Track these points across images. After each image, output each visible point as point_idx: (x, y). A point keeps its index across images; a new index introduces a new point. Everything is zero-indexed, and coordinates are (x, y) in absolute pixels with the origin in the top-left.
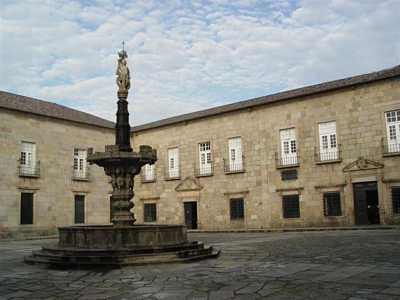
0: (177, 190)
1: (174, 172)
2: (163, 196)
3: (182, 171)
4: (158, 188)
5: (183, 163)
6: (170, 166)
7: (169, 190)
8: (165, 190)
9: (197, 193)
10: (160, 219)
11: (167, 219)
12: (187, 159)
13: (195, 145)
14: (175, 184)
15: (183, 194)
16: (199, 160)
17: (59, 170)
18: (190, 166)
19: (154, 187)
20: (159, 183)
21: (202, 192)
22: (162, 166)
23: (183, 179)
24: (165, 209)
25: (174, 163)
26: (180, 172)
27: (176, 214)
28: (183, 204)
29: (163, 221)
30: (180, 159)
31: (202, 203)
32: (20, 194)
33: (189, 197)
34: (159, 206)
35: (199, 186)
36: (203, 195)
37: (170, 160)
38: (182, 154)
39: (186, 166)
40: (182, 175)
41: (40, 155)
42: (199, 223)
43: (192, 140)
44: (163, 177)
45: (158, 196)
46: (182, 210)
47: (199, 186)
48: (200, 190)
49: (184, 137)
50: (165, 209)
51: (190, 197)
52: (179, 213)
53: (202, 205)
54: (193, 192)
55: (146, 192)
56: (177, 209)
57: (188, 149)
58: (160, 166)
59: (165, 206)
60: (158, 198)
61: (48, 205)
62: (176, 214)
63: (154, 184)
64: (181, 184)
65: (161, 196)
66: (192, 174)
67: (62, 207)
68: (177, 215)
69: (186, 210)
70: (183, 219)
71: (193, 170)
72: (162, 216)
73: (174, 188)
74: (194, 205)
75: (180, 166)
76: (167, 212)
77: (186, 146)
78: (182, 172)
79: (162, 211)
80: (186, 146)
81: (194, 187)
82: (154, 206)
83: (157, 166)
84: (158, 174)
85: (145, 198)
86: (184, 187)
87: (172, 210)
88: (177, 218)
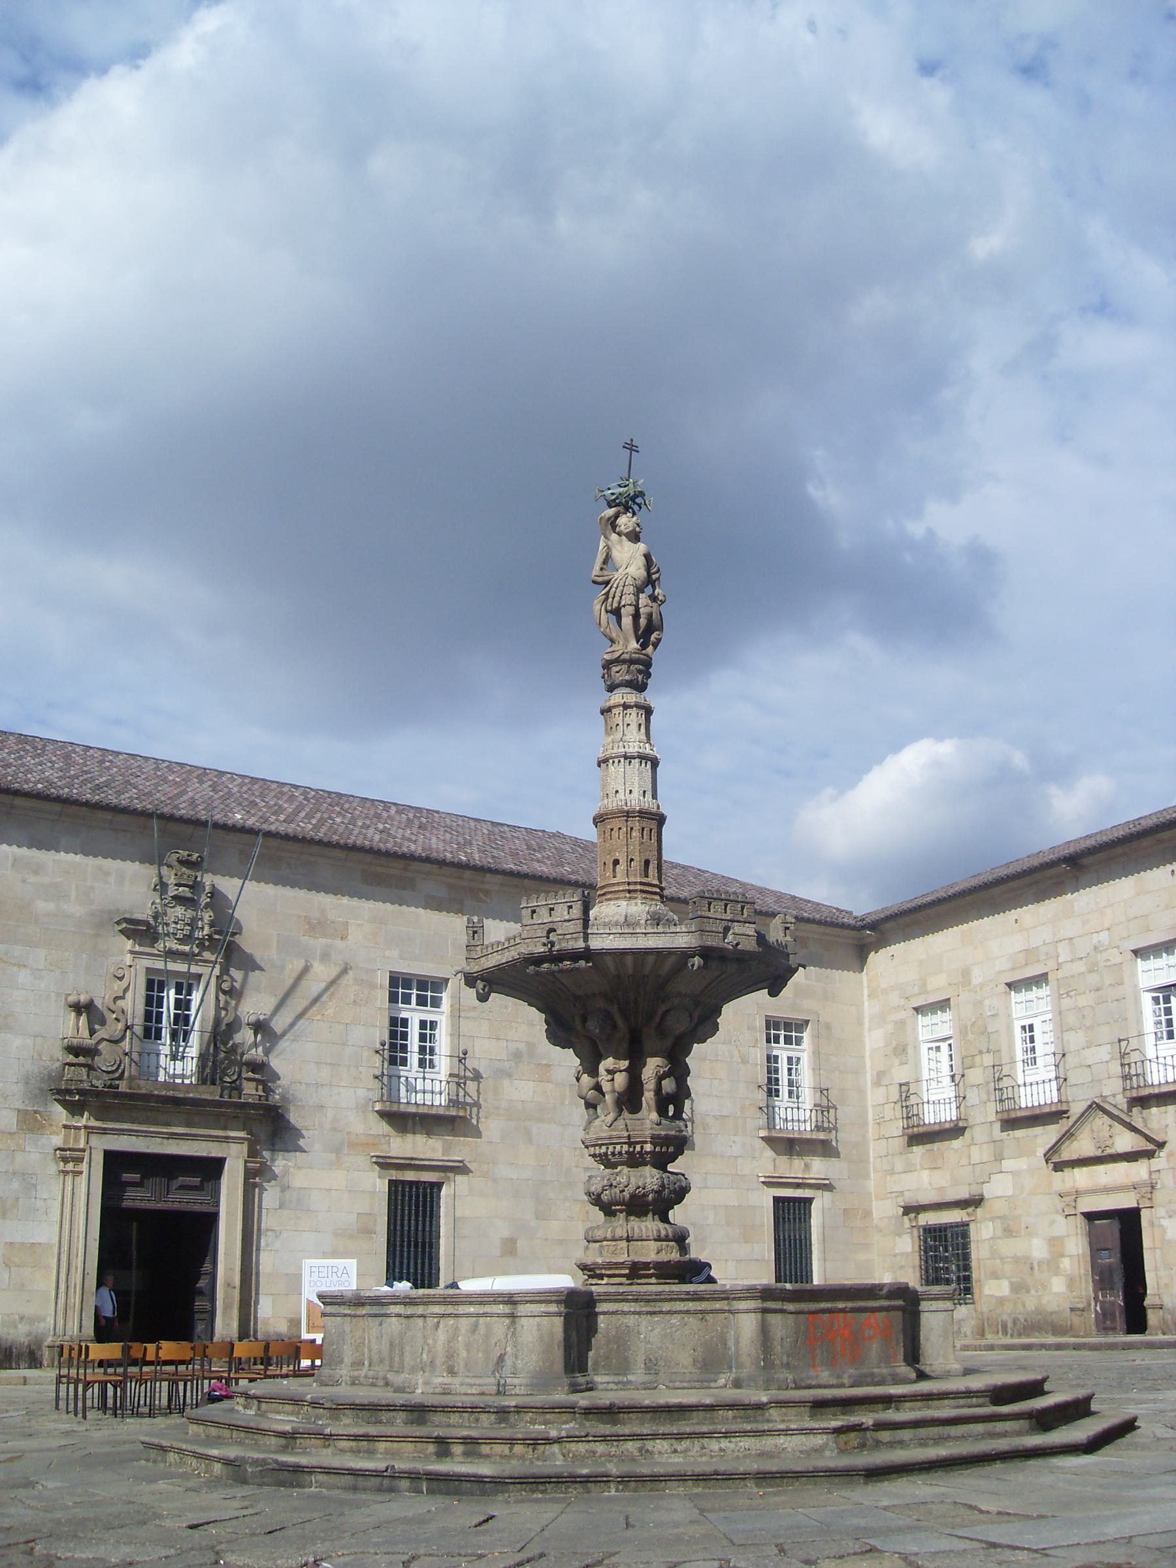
0: (1056, 1159)
1: (1036, 1088)
2: (997, 1188)
3: (1070, 1075)
4: (977, 1155)
5: (1075, 1040)
6: (1019, 1056)
7: (1021, 1164)
8: (1007, 1164)
9: (1139, 1171)
10: (987, 1291)
11: (1016, 1288)
12: (1088, 1023)
13: (1119, 959)
14: (1047, 1135)
15: (1080, 1177)
16: (1139, 1022)
17: (550, 1086)
18: (1104, 1052)
19: (956, 1151)
20: (977, 1133)
21: (1160, 1161)
22: (988, 1060)
23: (1076, 1109)
24: (1010, 1247)
25: (1038, 1044)
26: (1062, 1081)
27: (1052, 1264)
28: (1080, 1221)
29: (1001, 1301)
30: (1062, 1028)
31: (1160, 1211)
32: (383, 1186)
33: (1107, 1190)
34: (983, 1235)
35: (1148, 1138)
36: (1166, 1179)
37: (1018, 1034)
38: (1066, 1002)
39: (1087, 1052)
40: (1070, 1093)
41: (466, 1026)
42: (1154, 1307)
43: (1104, 937)
44: (992, 1107)
45: (975, 1190)
46: (1076, 1245)
47: (1148, 1138)
48: (1149, 1155)
49: (1070, 928)
50: (1010, 1247)
51: (1111, 1187)
52: (1066, 1263)
53: (1164, 1222)
54: (1123, 1166)
55: (925, 1174)
56: (1055, 1242)
57: (1093, 979)
58: (978, 1059)
59: (1008, 1232)
60: (975, 1202)
61: (502, 1230)
62: (1052, 1264)
63: (956, 1144)
64: (1068, 1135)
65: (988, 1191)
66: (1113, 1091)
67: (561, 1242)
68: (1057, 1273)
69: (1096, 1249)
70: (1087, 1288)
71: (1115, 1068)
72: (995, 1275)
73: (1040, 1152)
74: (1128, 1224)
75: (1062, 1055)
76: (1016, 1260)
77: (1080, 967)
78: (1070, 1081)
79: (995, 1254)
80: (1080, 967)
81: (1125, 1141)
82: (961, 1232)
83: (968, 1061)
84: (973, 1097)
85: (925, 1199)
86: (1084, 1146)
87: (1038, 1249)
88: (1058, 1285)
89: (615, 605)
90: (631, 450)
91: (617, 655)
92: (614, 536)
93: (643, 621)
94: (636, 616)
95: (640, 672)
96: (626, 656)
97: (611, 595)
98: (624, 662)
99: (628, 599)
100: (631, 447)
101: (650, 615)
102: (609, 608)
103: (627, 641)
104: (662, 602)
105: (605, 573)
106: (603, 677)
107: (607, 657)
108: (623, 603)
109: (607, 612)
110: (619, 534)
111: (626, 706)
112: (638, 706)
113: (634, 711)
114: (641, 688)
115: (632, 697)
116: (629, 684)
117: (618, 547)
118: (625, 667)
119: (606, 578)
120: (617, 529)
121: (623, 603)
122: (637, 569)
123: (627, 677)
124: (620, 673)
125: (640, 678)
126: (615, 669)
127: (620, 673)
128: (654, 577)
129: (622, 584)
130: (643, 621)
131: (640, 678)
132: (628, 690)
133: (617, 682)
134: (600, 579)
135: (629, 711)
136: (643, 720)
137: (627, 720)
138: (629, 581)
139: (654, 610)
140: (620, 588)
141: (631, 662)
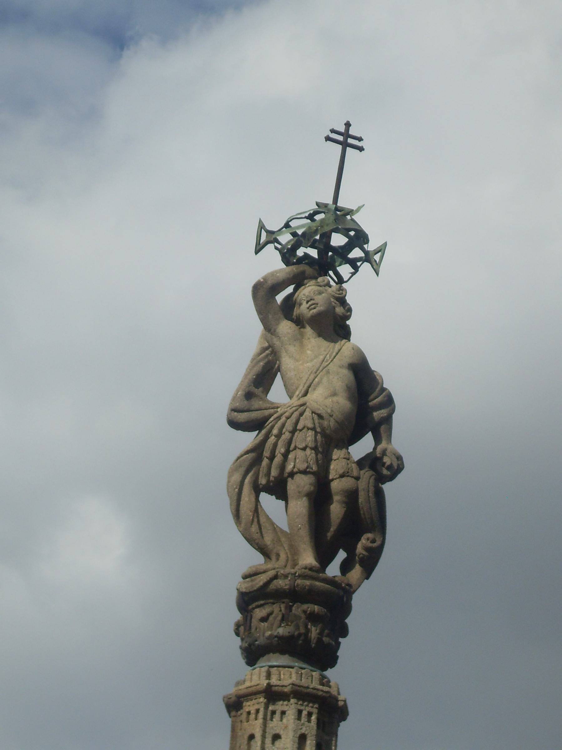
89: (274, 473)
90: (345, 145)
91: (262, 579)
92: (286, 327)
93: (336, 510)
94: (320, 498)
95: (313, 618)
96: (281, 583)
97: (267, 453)
98: (278, 596)
99: (299, 459)
100: (345, 140)
101: (352, 496)
102: (263, 481)
103: (295, 553)
104: (396, 470)
105: (256, 403)
106: (237, 634)
107: (246, 586)
108: (289, 467)
109: (257, 489)
110: (299, 322)
111: (272, 695)
112: (300, 694)
113: (291, 707)
114: (323, 657)
115: (310, 678)
116: (287, 646)
117: (292, 349)
118: (278, 609)
119: (254, 415)
120: (296, 312)
121: (289, 467)
122: (329, 396)
123: (281, 631)
124: (272, 624)
125: (314, 631)
126: (259, 613)
127: (272, 624)
128: (377, 415)
129: (289, 426)
130: (336, 510)
131: (314, 631)
132: (284, 660)
133: (261, 641)
134: (242, 417)
135: (280, 706)
136: (311, 728)
137: (275, 725)
138: (306, 420)
139: (362, 485)
140: (286, 436)
141: (294, 596)
